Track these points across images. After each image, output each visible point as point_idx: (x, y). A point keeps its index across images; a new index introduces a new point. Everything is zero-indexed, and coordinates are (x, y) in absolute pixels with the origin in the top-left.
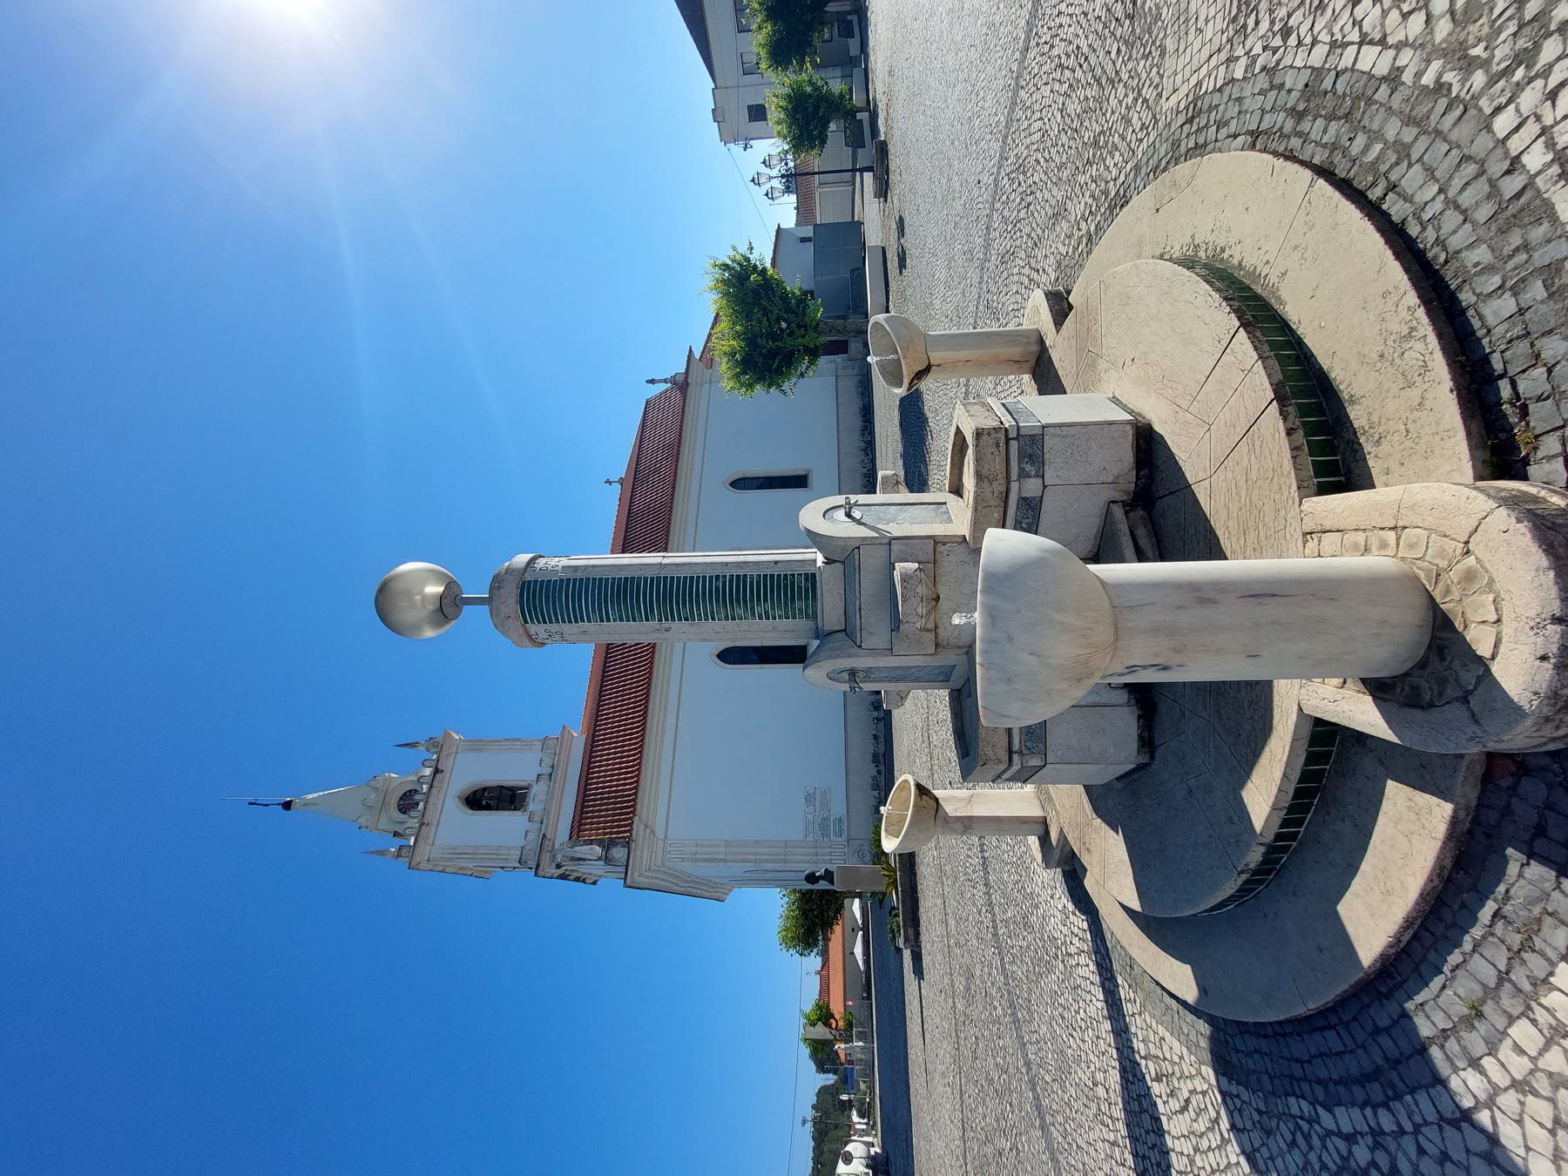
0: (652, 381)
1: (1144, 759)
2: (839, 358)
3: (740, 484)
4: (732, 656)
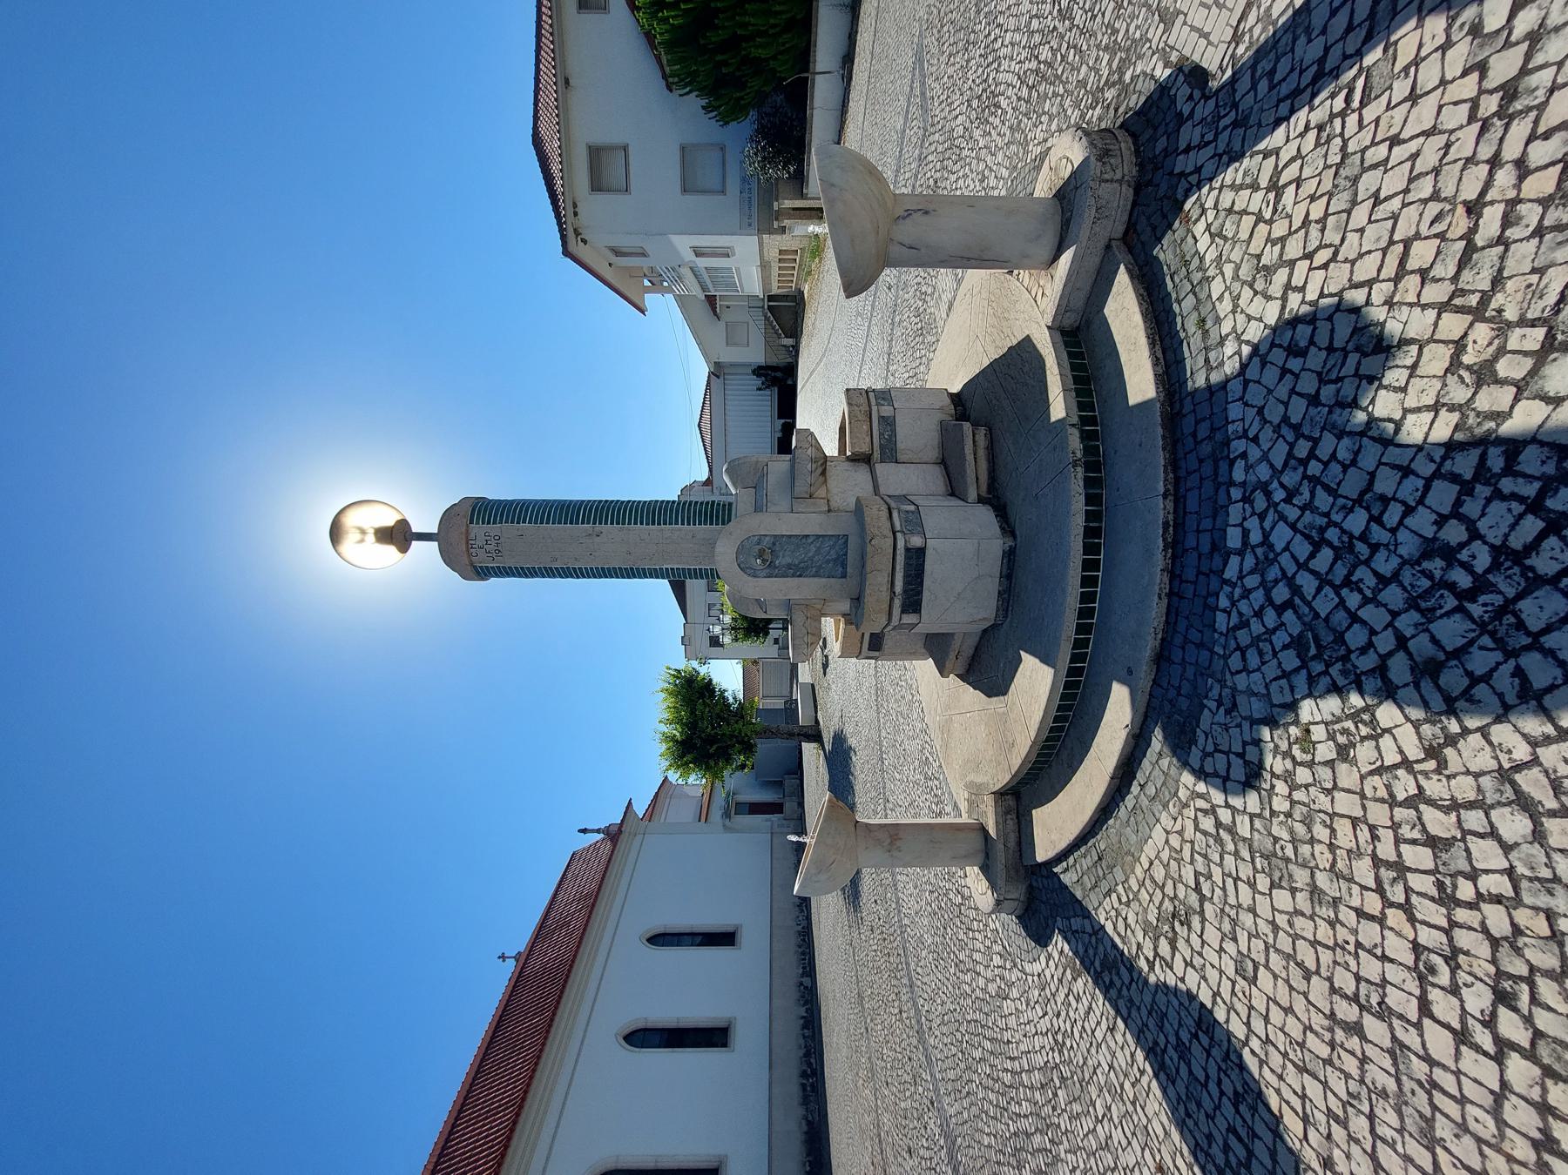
0: (584, 831)
1: (1010, 543)
2: (775, 817)
3: (660, 939)
4: (681, 95)
